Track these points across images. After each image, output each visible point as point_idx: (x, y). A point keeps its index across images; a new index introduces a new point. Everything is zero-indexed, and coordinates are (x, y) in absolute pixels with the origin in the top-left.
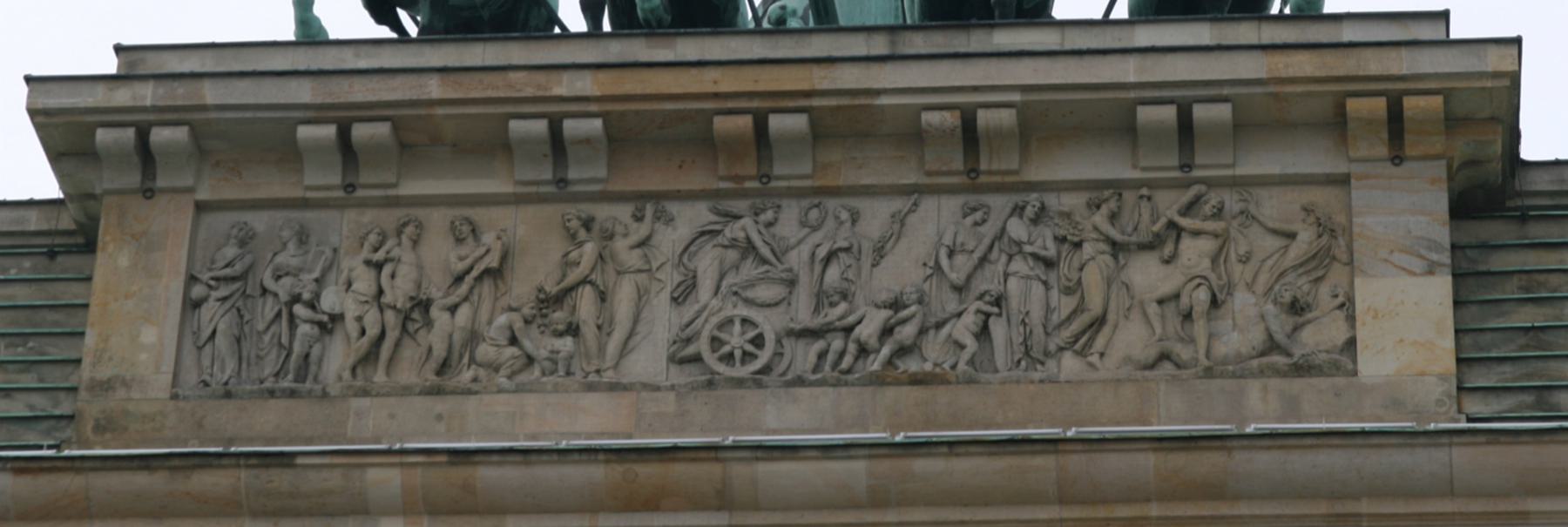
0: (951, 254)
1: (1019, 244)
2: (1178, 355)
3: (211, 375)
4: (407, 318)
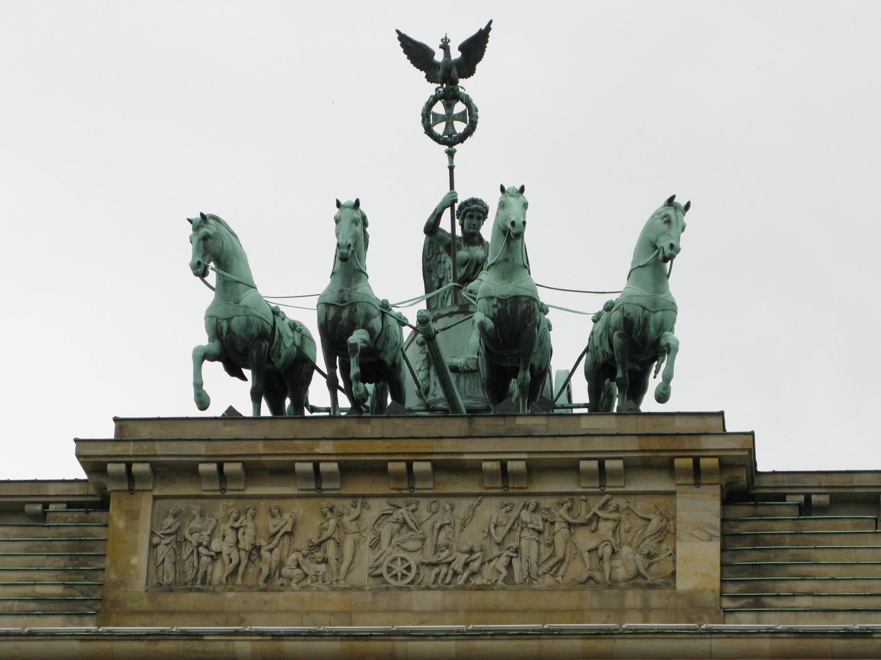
1: (526, 523)
2: (596, 578)
4: (250, 554)
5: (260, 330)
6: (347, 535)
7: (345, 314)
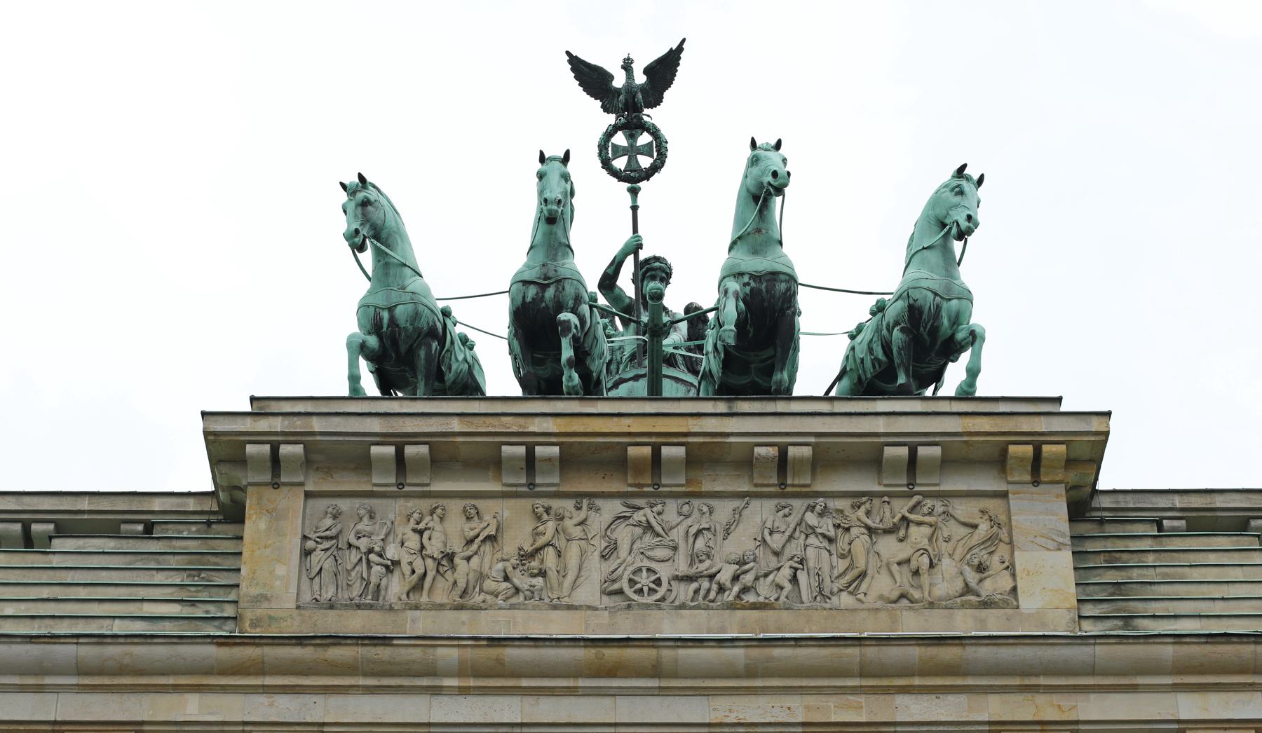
0: (771, 533)
1: (812, 528)
2: (912, 595)
4: (439, 564)
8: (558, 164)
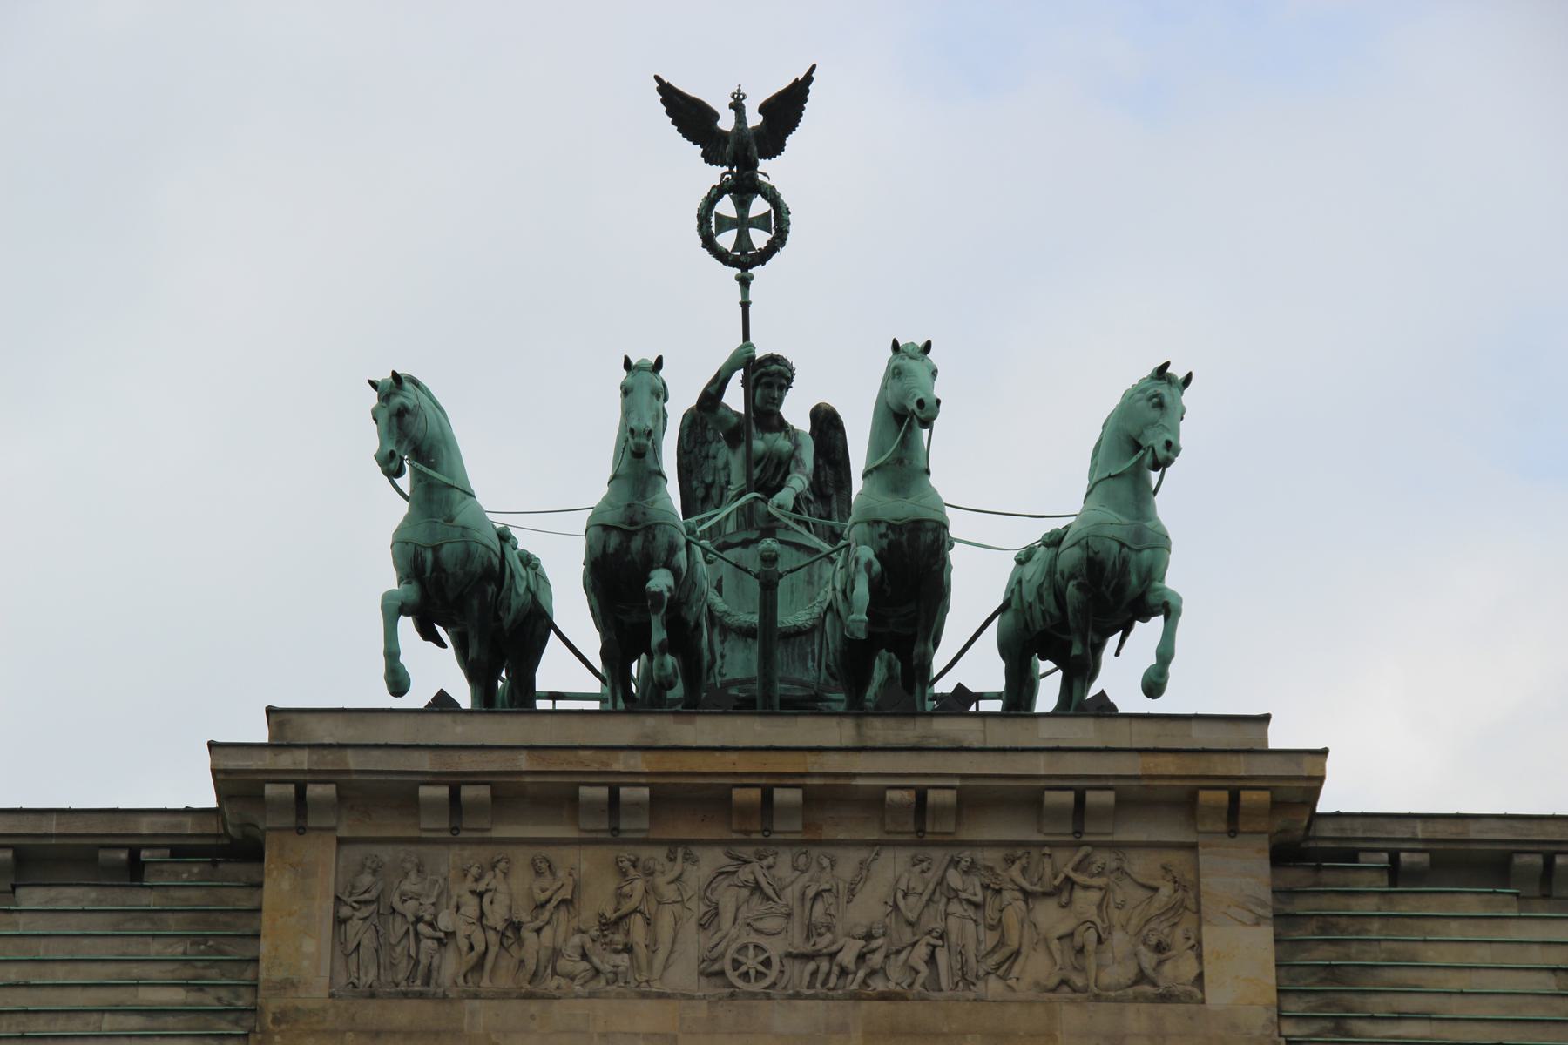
0: (905, 895)
1: (956, 891)
3: (358, 979)
4: (503, 934)
5: (485, 565)
6: (661, 906)
7: (637, 543)
8: (647, 375)
